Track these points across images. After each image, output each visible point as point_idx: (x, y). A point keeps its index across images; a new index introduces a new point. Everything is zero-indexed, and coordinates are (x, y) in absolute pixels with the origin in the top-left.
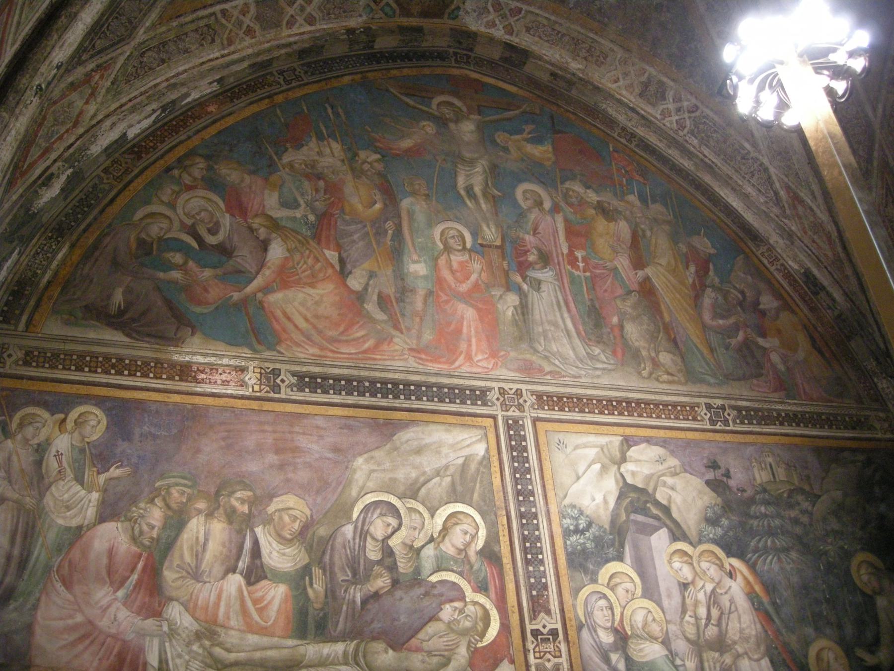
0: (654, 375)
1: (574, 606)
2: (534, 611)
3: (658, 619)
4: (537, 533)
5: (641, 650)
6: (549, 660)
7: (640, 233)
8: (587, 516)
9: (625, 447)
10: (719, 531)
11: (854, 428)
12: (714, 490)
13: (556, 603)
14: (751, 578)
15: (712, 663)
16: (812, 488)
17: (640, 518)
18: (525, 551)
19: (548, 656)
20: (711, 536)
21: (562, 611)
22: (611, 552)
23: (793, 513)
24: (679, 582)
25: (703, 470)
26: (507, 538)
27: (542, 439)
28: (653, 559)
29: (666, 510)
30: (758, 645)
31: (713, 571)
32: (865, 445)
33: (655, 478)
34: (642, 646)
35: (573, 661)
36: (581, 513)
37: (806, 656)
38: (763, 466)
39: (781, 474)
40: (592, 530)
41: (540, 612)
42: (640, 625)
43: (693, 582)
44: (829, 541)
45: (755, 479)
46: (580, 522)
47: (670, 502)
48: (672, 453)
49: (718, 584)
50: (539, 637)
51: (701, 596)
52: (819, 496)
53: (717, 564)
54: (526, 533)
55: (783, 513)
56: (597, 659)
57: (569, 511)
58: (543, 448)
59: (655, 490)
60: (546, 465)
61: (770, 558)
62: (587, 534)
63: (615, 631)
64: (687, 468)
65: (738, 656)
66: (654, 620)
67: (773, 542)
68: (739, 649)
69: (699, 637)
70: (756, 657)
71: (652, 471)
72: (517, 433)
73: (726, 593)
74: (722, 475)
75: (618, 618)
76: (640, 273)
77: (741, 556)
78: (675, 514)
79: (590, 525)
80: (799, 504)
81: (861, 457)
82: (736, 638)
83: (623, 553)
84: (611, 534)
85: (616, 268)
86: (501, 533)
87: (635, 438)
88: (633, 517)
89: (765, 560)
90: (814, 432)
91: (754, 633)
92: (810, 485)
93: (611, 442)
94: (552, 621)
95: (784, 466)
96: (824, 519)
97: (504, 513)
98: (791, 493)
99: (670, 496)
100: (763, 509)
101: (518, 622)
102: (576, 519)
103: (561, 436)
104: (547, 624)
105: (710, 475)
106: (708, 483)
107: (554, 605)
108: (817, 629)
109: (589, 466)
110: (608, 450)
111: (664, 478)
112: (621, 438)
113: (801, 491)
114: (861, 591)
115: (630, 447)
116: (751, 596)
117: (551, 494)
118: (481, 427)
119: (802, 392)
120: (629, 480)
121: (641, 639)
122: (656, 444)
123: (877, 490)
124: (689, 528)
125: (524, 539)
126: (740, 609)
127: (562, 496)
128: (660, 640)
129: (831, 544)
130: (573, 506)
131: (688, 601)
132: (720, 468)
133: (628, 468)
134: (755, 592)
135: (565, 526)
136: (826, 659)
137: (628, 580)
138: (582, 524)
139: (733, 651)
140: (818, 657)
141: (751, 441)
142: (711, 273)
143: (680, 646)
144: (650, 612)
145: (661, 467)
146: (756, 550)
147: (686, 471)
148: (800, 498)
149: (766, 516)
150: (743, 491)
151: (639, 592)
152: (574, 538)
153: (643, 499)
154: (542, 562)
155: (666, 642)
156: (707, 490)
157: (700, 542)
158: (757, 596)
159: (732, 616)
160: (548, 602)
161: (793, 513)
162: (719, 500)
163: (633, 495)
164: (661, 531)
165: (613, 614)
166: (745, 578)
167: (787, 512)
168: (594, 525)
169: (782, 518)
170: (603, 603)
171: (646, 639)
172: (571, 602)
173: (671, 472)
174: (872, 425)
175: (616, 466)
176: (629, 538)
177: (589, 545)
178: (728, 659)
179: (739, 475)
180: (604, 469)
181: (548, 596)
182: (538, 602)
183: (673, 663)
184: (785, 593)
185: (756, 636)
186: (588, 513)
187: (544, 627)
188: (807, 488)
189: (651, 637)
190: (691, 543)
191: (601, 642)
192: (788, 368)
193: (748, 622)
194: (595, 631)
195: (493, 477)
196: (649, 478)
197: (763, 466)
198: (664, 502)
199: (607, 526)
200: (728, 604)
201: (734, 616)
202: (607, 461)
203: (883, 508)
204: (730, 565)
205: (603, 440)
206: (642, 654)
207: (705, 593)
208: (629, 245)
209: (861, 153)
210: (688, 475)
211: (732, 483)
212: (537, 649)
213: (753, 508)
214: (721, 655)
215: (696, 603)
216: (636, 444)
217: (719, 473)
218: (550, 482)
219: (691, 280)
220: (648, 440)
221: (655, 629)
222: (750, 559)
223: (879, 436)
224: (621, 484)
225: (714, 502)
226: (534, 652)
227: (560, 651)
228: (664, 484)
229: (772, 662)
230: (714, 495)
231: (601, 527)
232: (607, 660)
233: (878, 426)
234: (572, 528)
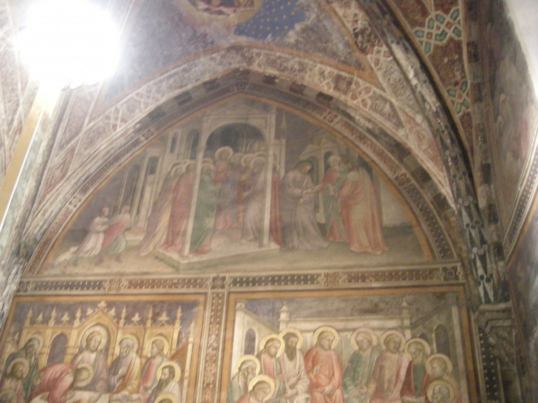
209: (67, 135)
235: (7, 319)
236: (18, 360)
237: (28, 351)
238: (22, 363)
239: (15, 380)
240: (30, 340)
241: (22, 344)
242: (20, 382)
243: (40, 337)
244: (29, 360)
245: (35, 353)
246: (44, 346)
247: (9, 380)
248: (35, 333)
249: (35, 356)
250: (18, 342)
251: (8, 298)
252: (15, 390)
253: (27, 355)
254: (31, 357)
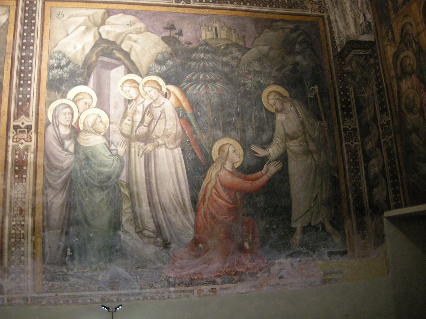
1: (46, 112)
2: (18, 114)
3: (104, 121)
4: (30, 68)
5: (87, 139)
6: (22, 143)
8: (68, 58)
9: (106, 15)
10: (164, 68)
11: (290, 7)
12: (167, 43)
13: (34, 110)
14: (181, 98)
15: (137, 150)
16: (245, 44)
17: (106, 59)
18: (20, 78)
19: (22, 141)
20: (157, 71)
21: (37, 114)
22: (80, 79)
23: (225, 59)
24: (125, 99)
25: (162, 30)
26: (9, 71)
27: (47, 12)
28: (109, 84)
29: (127, 55)
30: (175, 140)
31: (154, 93)
32: (296, 18)
33: (124, 35)
34: (88, 137)
35: (39, 144)
36: (64, 56)
37: (211, 149)
38: (210, 29)
39: (223, 34)
40: (71, 66)
41: (21, 115)
42: (90, 125)
43: (136, 99)
44: (250, 77)
45: (201, 37)
46: (62, 61)
47: (131, 50)
48: (141, 20)
49: (154, 101)
50: (18, 130)
51: (140, 108)
52: (249, 49)
53: (157, 89)
54: (23, 68)
55: (217, 58)
56: (55, 144)
57: (56, 55)
58: (47, 17)
59: (122, 42)
60: (47, 27)
61: (199, 86)
62: (65, 69)
63: (72, 127)
64: (150, 29)
65: (159, 145)
66: (101, 121)
67: (205, 76)
68: (160, 141)
69: (132, 133)
70: (172, 147)
71: (123, 31)
72: (31, 9)
73: (159, 107)
74: (176, 34)
75: (75, 120)
77: (177, 84)
78: (133, 57)
79: (68, 63)
80: (231, 53)
81: (291, 26)
82: (160, 135)
83: (88, 80)
84: (82, 69)
86: (5, 68)
87: (115, 11)
88: (101, 58)
89: (196, 87)
90: (257, 9)
91: (174, 132)
92: (245, 42)
93: (96, 13)
94: (29, 120)
95: (226, 29)
96: (249, 64)
97: (10, 56)
98: (227, 46)
99: (132, 46)
100: (202, 56)
101: (6, 121)
102: (60, 60)
103: (61, 10)
104: (25, 122)
105: (167, 34)
106: (163, 39)
107: (32, 111)
108: (224, 131)
109: (77, 28)
110: (93, 18)
111: (130, 35)
112: (105, 10)
113: (237, 45)
114: (266, 110)
115: (109, 15)
116: (179, 109)
117: (45, 45)
118: (7, 6)
120: (104, 36)
121: (89, 132)
122: (130, 14)
123: (297, 47)
124: (141, 66)
125: (21, 71)
126: (168, 118)
127: (53, 45)
128: (102, 134)
129: (251, 79)
130: (59, 52)
131: (129, 111)
132: (175, 29)
133: (104, 30)
134: (182, 106)
135: (51, 64)
136: (226, 150)
137: (89, 97)
138: (63, 62)
139: (156, 143)
140: (221, 149)
141: (205, 13)
143: (116, 138)
144: (99, 116)
145: (130, 28)
146: (190, 80)
147: (148, 31)
148: (234, 49)
149: (203, 60)
150: (190, 43)
151: (95, 103)
152: (55, 71)
153: (111, 47)
154: (30, 85)
155: (106, 135)
156: (162, 42)
157: (147, 75)
158: (183, 109)
159: (160, 121)
160: (29, 109)
161: (225, 59)
162: (169, 49)
163: (104, 45)
164: (120, 67)
165: (73, 117)
166: (177, 98)
167: (221, 58)
168: (71, 63)
169: (216, 61)
170: (67, 110)
171: (93, 133)
172: (44, 110)
173: (137, 31)
174: (305, 6)
175: (97, 28)
176: (95, 71)
177: (65, 75)
178: (150, 147)
179: (189, 34)
180: (88, 29)
181: (29, 106)
182: (22, 109)
183: (109, 148)
184: (205, 108)
185: (176, 134)
186: (69, 56)
187: (23, 124)
188: (241, 43)
189: (96, 132)
190: (140, 75)
191: (60, 133)
193: (172, 125)
194: (58, 127)
195: (8, 35)
196: (119, 35)
197: (210, 29)
198: (127, 50)
199: (80, 64)
200: (159, 114)
201: (162, 121)
202: (90, 24)
203: (298, 58)
204: (167, 89)
205: (91, 12)
206: (87, 142)
207: (144, 106)
210: (149, 33)
211: (183, 39)
212: (16, 137)
213: (194, 55)
214: (145, 144)
215: (135, 113)
216: (115, 14)
217: (173, 33)
218: (48, 38)
220: (124, 12)
221: (101, 127)
222: (184, 86)
223: (310, 13)
224: (97, 39)
225: (164, 50)
226: (13, 138)
227: (31, 138)
228: (130, 39)
229: (183, 150)
230: (166, 46)
231: (75, 65)
232: (62, 144)
233: (309, 6)
234: (55, 65)
235: (375, 26)
236: (401, 56)
237: (406, 41)
238: (407, 56)
239: (408, 77)
240: (402, 30)
241: (398, 38)
242: (413, 76)
243: (409, 19)
244: (411, 49)
245: (413, 38)
246: (417, 25)
247: (404, 81)
248: (403, 19)
249: (415, 41)
250: (394, 39)
251: (365, 6)
252: (413, 88)
253: (406, 45)
254: (411, 46)
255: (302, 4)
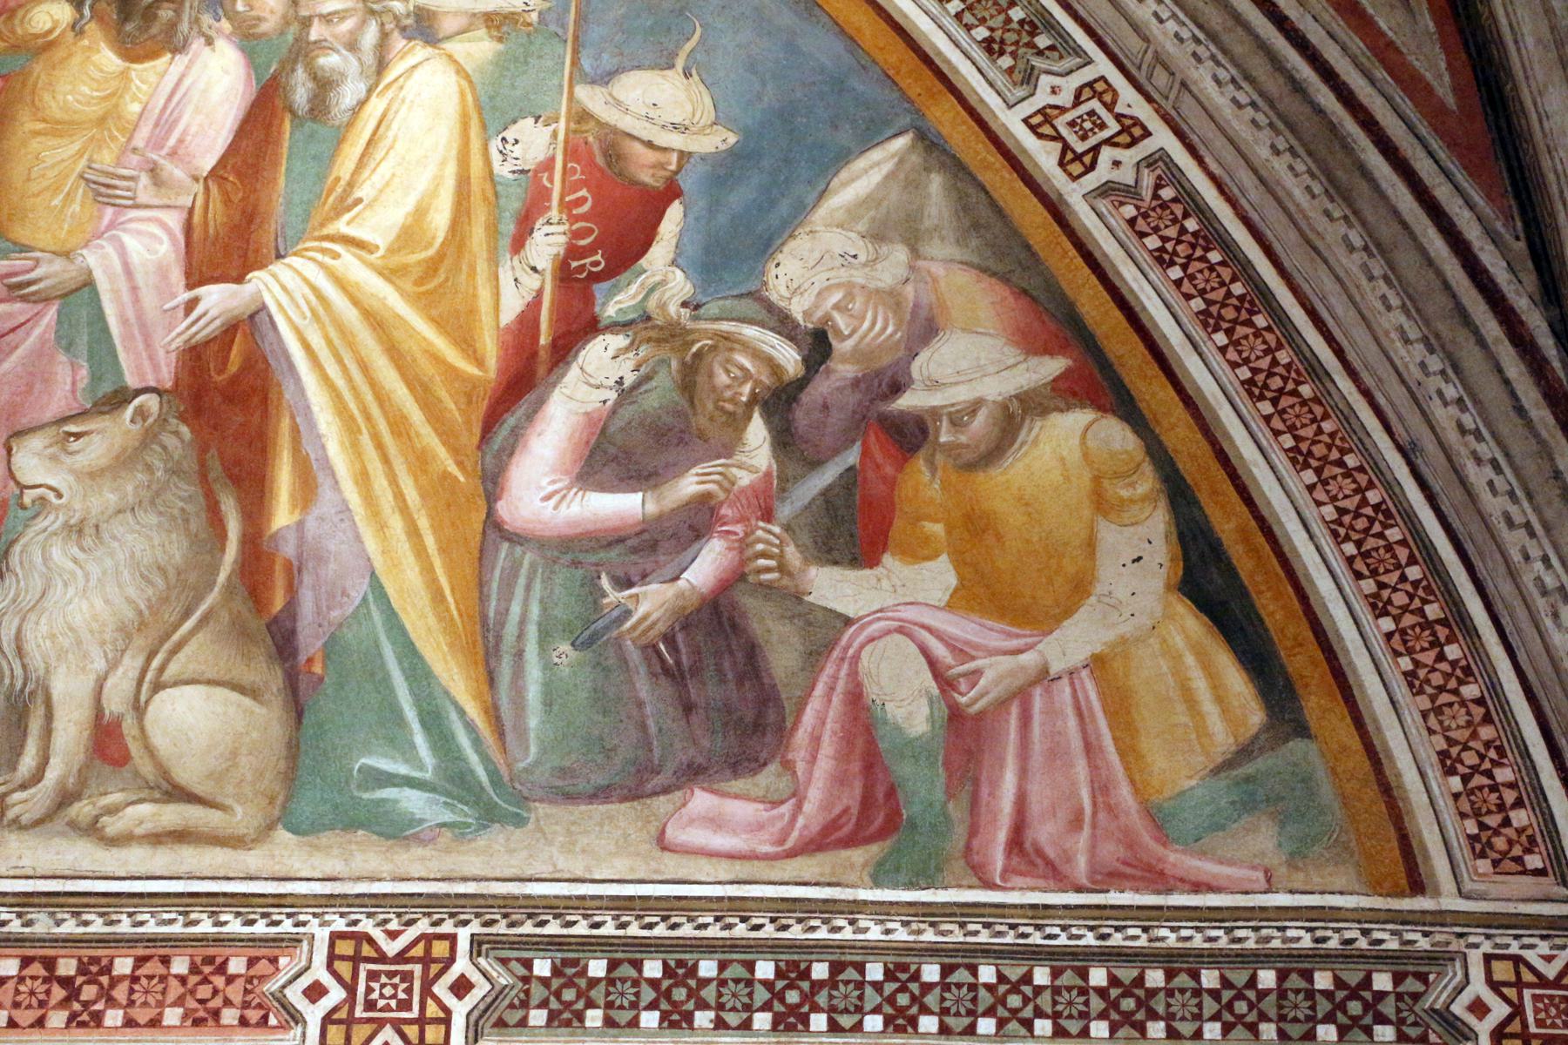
0: (82, 810)
7: (301, 91)
76: (218, 299)
85: (88, 283)
119: (1002, 836)
142: (659, 256)
192: (956, 716)
208: (207, 163)
219: (512, 305)
255: (1416, 997)
